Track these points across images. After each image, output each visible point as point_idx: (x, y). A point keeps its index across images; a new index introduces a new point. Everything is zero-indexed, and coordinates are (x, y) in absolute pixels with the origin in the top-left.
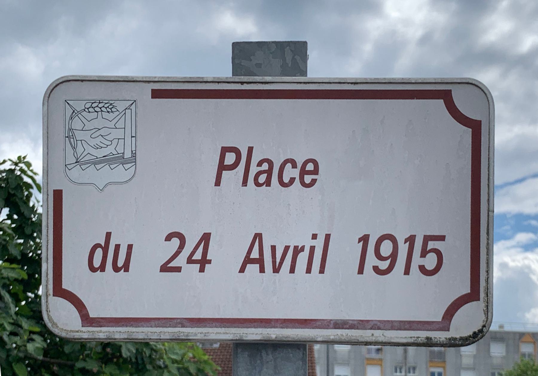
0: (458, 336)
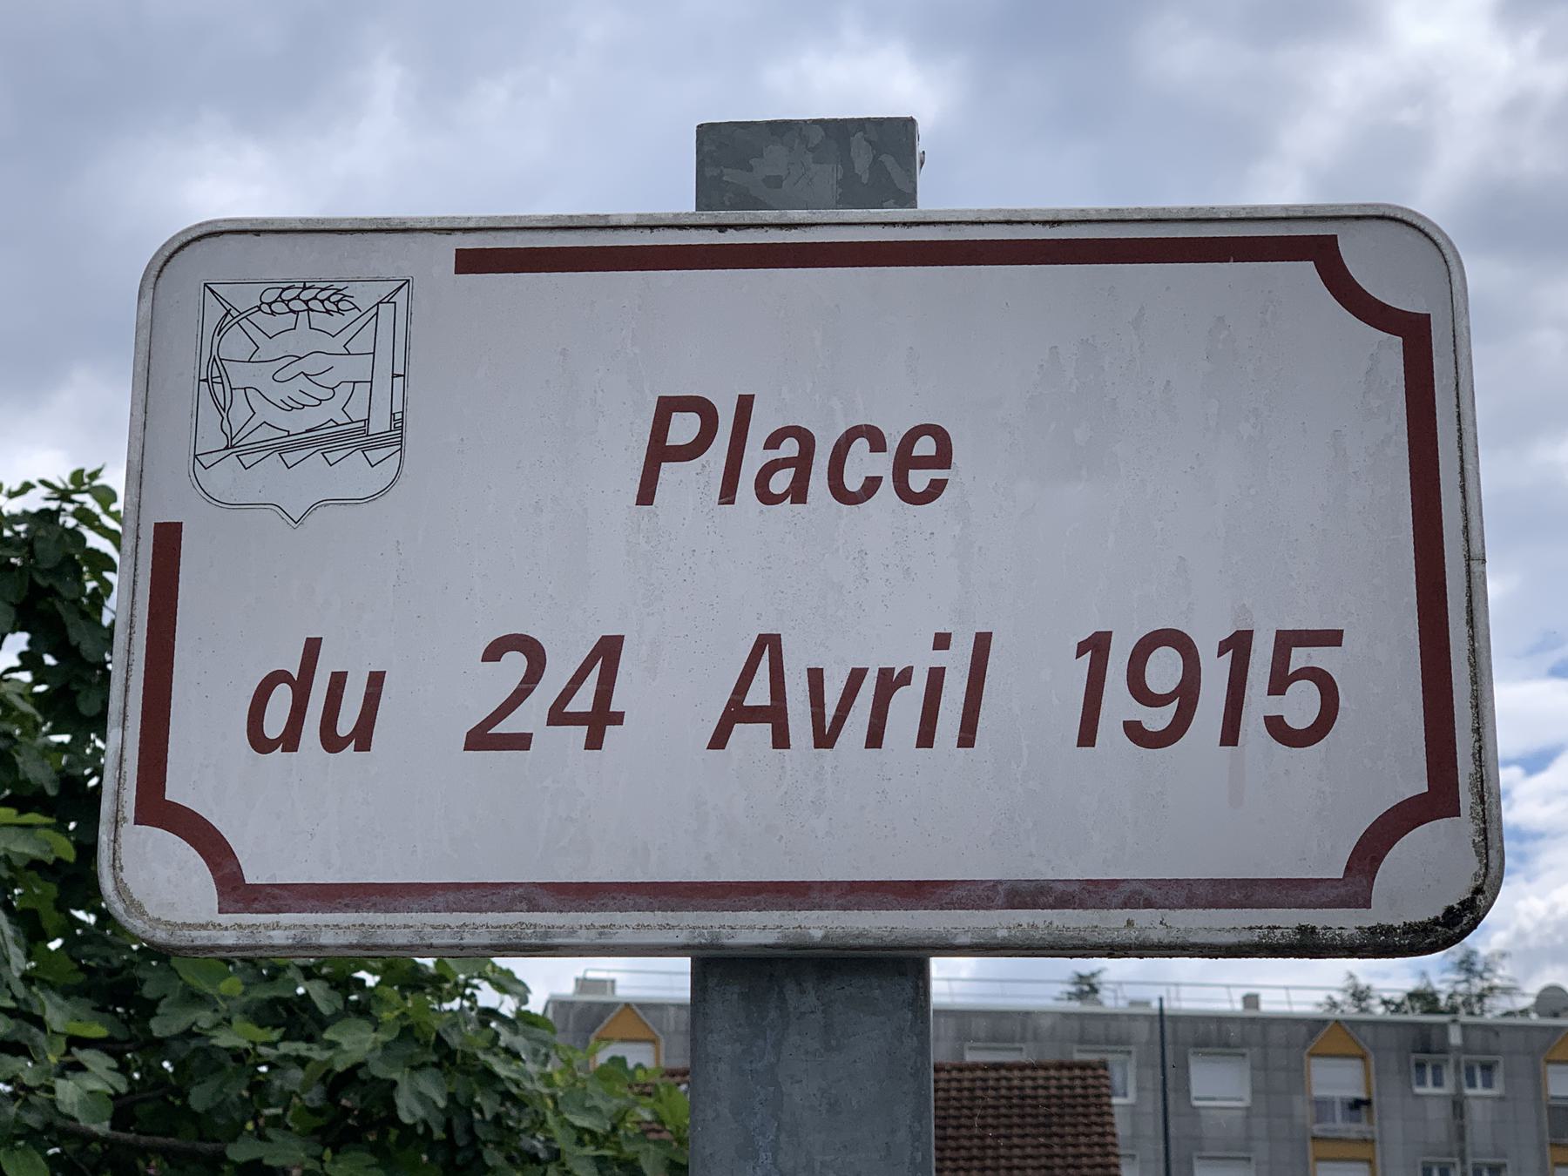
0: (1397, 923)
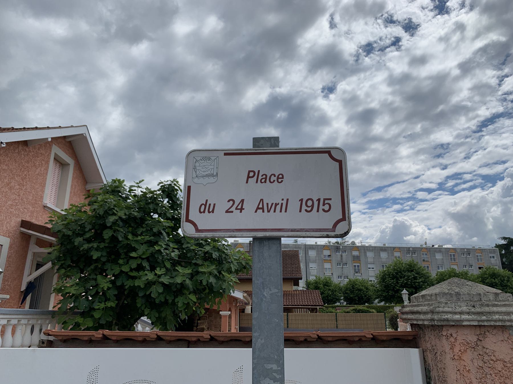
0: (339, 234)
